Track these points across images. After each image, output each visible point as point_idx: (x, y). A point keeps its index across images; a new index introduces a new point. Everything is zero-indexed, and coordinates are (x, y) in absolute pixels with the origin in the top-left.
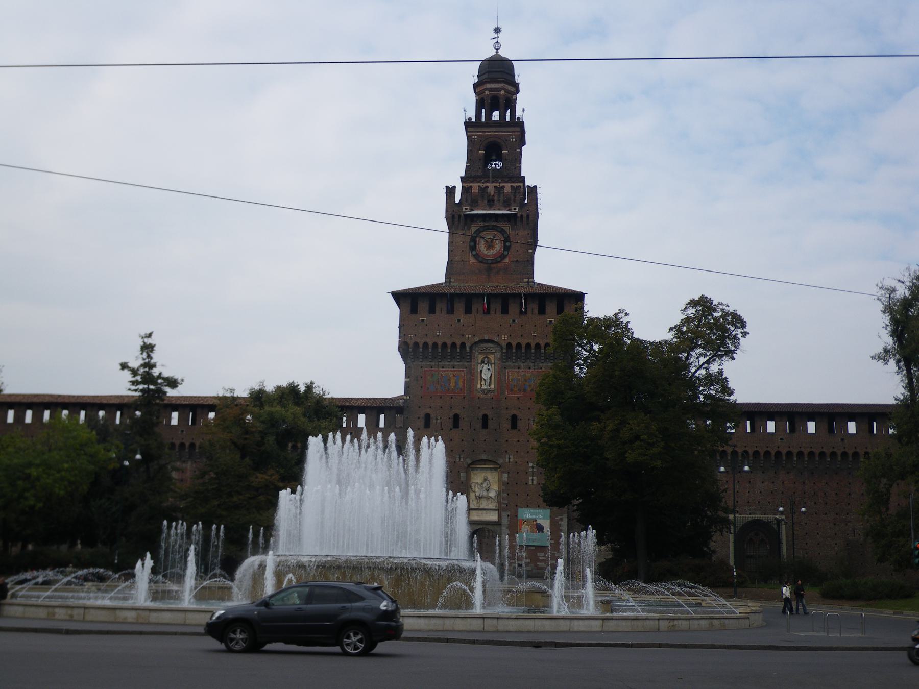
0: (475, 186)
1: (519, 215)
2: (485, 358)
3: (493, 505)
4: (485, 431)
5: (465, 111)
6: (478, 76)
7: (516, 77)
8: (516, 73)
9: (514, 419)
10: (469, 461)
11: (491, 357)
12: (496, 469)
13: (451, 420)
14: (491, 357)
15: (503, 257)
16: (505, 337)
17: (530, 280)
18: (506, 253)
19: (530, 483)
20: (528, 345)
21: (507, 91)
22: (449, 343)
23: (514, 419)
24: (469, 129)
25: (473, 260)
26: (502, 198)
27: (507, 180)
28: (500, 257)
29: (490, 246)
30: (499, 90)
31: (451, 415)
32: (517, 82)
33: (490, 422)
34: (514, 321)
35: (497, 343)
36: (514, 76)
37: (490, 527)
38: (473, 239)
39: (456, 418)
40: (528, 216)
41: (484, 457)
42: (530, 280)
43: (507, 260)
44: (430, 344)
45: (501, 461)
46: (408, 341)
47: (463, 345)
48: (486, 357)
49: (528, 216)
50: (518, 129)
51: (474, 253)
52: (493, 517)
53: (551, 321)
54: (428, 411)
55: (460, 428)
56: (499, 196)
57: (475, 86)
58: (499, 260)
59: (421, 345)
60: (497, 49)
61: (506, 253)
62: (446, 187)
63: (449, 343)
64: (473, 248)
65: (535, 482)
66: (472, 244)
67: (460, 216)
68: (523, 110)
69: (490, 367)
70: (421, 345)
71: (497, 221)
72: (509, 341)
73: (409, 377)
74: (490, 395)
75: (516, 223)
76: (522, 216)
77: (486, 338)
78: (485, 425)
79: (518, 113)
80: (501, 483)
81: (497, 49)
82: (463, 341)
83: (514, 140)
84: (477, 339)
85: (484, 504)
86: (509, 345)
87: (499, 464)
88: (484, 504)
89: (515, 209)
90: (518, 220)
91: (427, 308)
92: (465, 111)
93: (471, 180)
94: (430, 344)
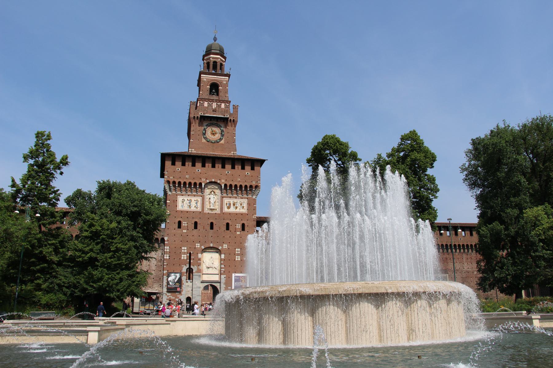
0: (206, 104)
1: (229, 119)
2: (212, 191)
3: (217, 272)
4: (211, 230)
5: (200, 66)
6: (206, 52)
7: (225, 54)
8: (225, 52)
9: (228, 225)
10: (203, 247)
11: (215, 191)
12: (217, 252)
13: (193, 225)
14: (215, 191)
15: (221, 139)
16: (223, 181)
17: (235, 152)
18: (222, 138)
19: (237, 259)
20: (236, 186)
21: (221, 60)
22: (193, 182)
23: (228, 225)
24: (202, 75)
25: (204, 141)
26: (220, 110)
27: (221, 102)
28: (219, 139)
29: (213, 134)
30: (218, 58)
31: (193, 223)
32: (225, 55)
33: (214, 226)
34: (228, 172)
35: (219, 185)
36: (224, 54)
37: (213, 284)
38: (205, 130)
39: (196, 224)
40: (234, 120)
41: (211, 245)
42: (235, 152)
43: (222, 142)
44: (182, 183)
45: (220, 248)
46: (170, 180)
47: (200, 184)
48: (213, 191)
49: (234, 120)
50: (228, 78)
51: (205, 136)
52: (216, 278)
53: (248, 173)
54: (180, 219)
55: (198, 229)
56: (218, 108)
57: (204, 56)
58: (218, 141)
59: (177, 183)
60: (215, 41)
61: (222, 138)
62: (191, 101)
63: (193, 182)
64: (204, 134)
65: (239, 259)
66: (204, 132)
67: (198, 117)
68: (230, 69)
69: (215, 196)
70: (177, 183)
71: (217, 121)
72: (225, 183)
73: (169, 200)
74: (214, 212)
75: (227, 123)
76: (230, 120)
77: (213, 180)
78: (212, 227)
79: (226, 71)
80: (221, 260)
81: (215, 41)
82: (201, 181)
83: (225, 83)
84: (208, 181)
85: (210, 271)
86: (226, 185)
87: (219, 249)
88: (210, 271)
89: (227, 116)
90: (229, 121)
91: (181, 163)
92: (200, 66)
93: (203, 100)
94: (182, 183)
